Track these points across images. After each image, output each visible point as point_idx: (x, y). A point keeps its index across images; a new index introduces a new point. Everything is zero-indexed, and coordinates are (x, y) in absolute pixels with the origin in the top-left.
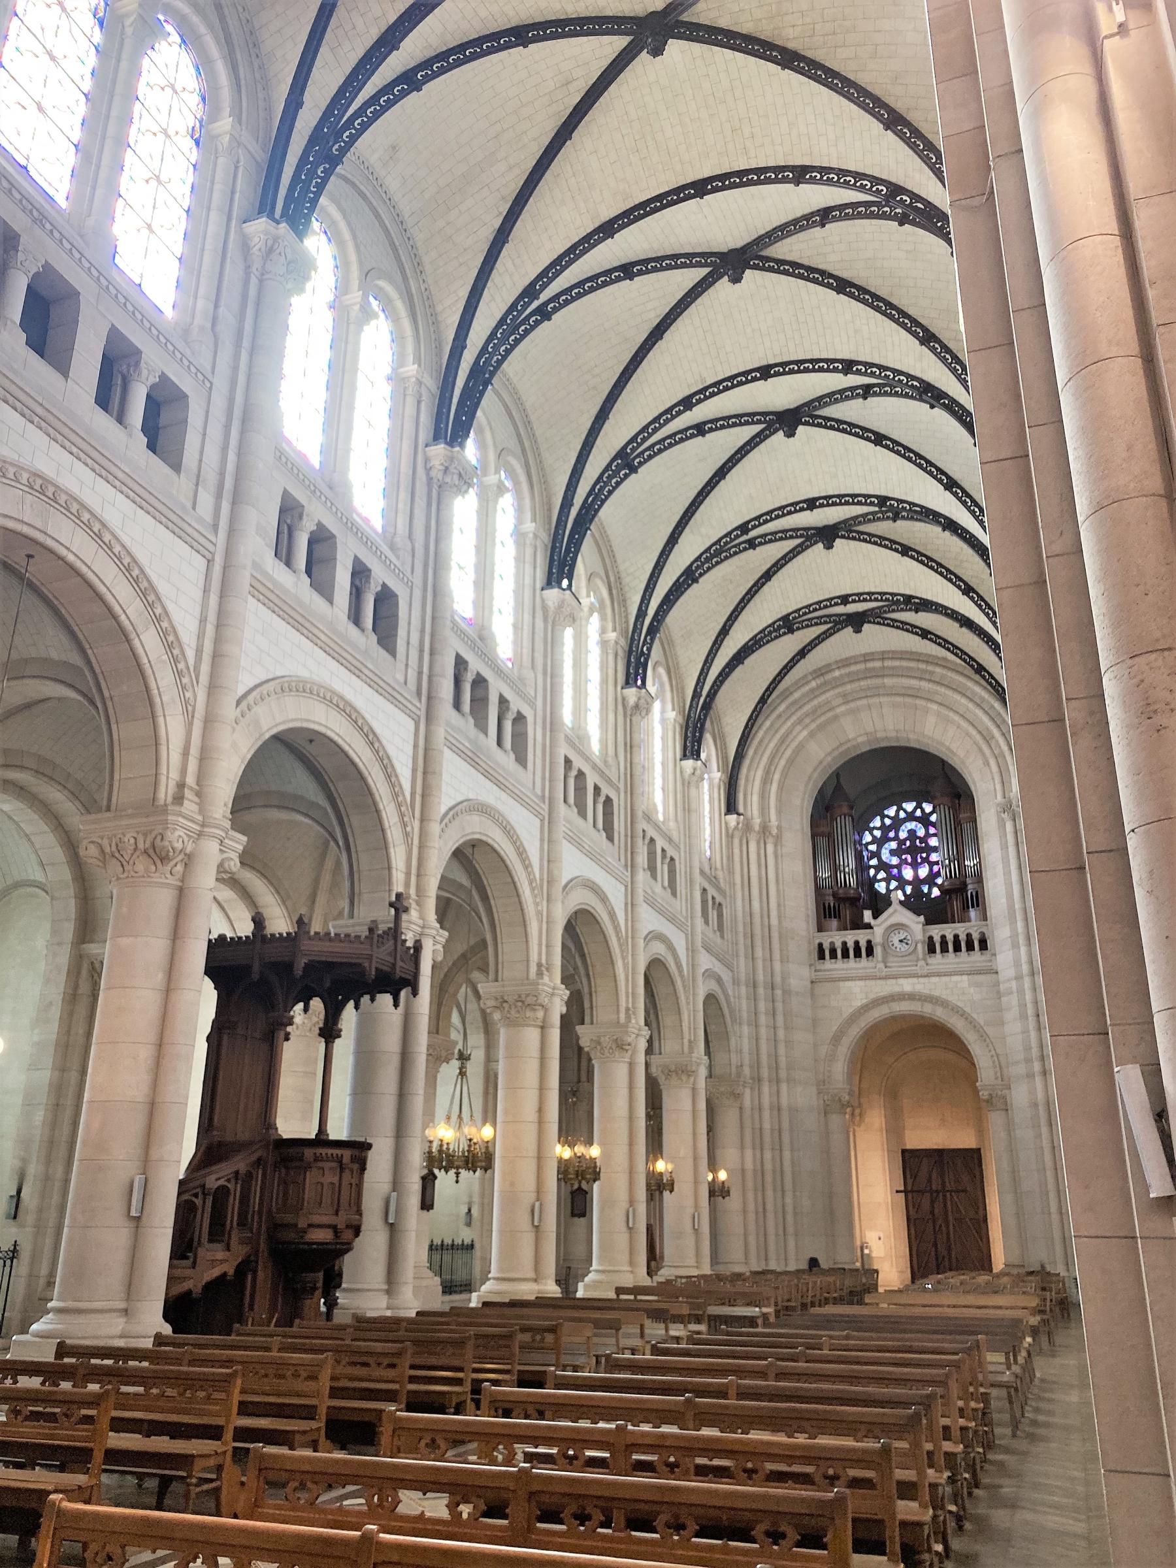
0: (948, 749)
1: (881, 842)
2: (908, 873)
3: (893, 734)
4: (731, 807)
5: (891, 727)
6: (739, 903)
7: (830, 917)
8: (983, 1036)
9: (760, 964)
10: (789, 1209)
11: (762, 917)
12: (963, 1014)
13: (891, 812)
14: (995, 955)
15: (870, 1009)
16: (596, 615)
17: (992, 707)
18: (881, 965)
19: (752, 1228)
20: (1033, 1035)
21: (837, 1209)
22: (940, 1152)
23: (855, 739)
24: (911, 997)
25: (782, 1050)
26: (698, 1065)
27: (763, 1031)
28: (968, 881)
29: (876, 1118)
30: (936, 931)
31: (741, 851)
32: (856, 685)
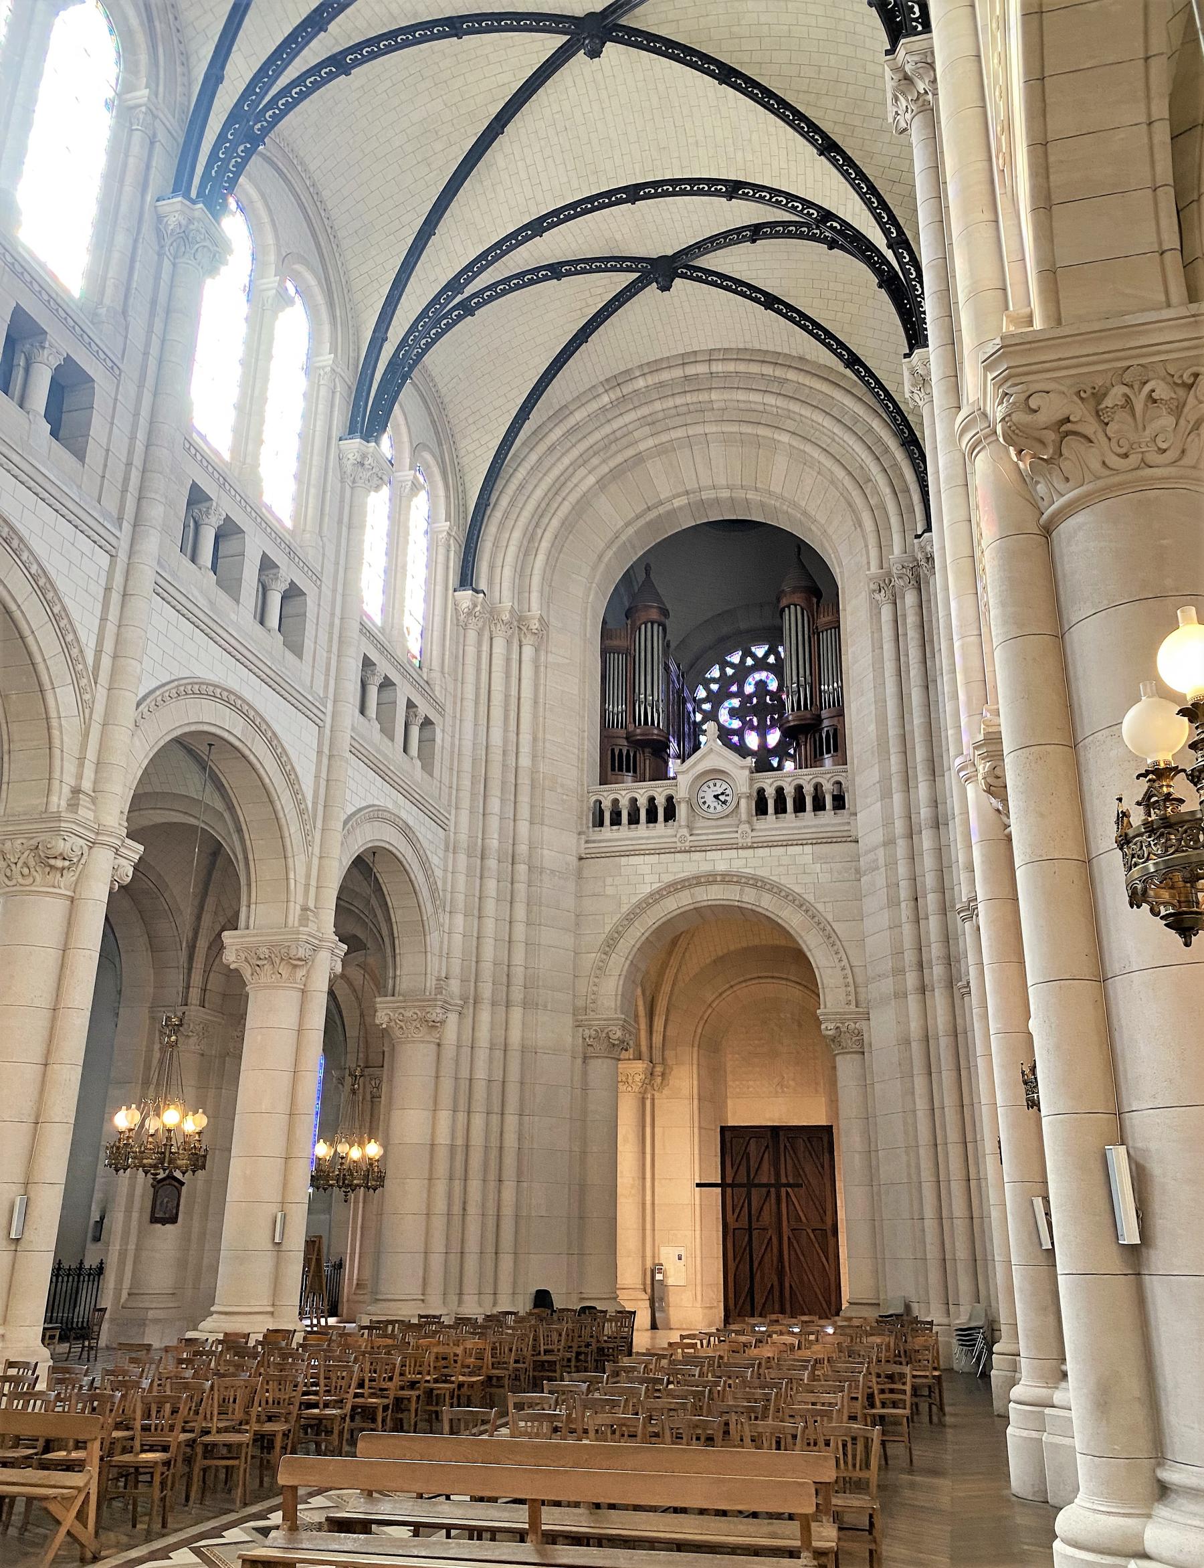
0: (805, 513)
1: (716, 700)
2: (752, 740)
3: (725, 494)
4: (466, 579)
5: (724, 483)
6: (468, 726)
7: (621, 769)
8: (830, 937)
9: (494, 823)
10: (508, 1211)
11: (504, 753)
12: (801, 904)
13: (735, 658)
14: (856, 814)
15: (662, 897)
16: (423, 495)
17: (871, 430)
18: (685, 831)
19: (438, 1245)
20: (907, 929)
21: (589, 1215)
22: (775, 1130)
23: (669, 500)
24: (726, 879)
25: (519, 957)
26: (316, 949)
27: (489, 926)
28: (825, 713)
29: (685, 1080)
30: (769, 783)
31: (479, 652)
32: (670, 403)
